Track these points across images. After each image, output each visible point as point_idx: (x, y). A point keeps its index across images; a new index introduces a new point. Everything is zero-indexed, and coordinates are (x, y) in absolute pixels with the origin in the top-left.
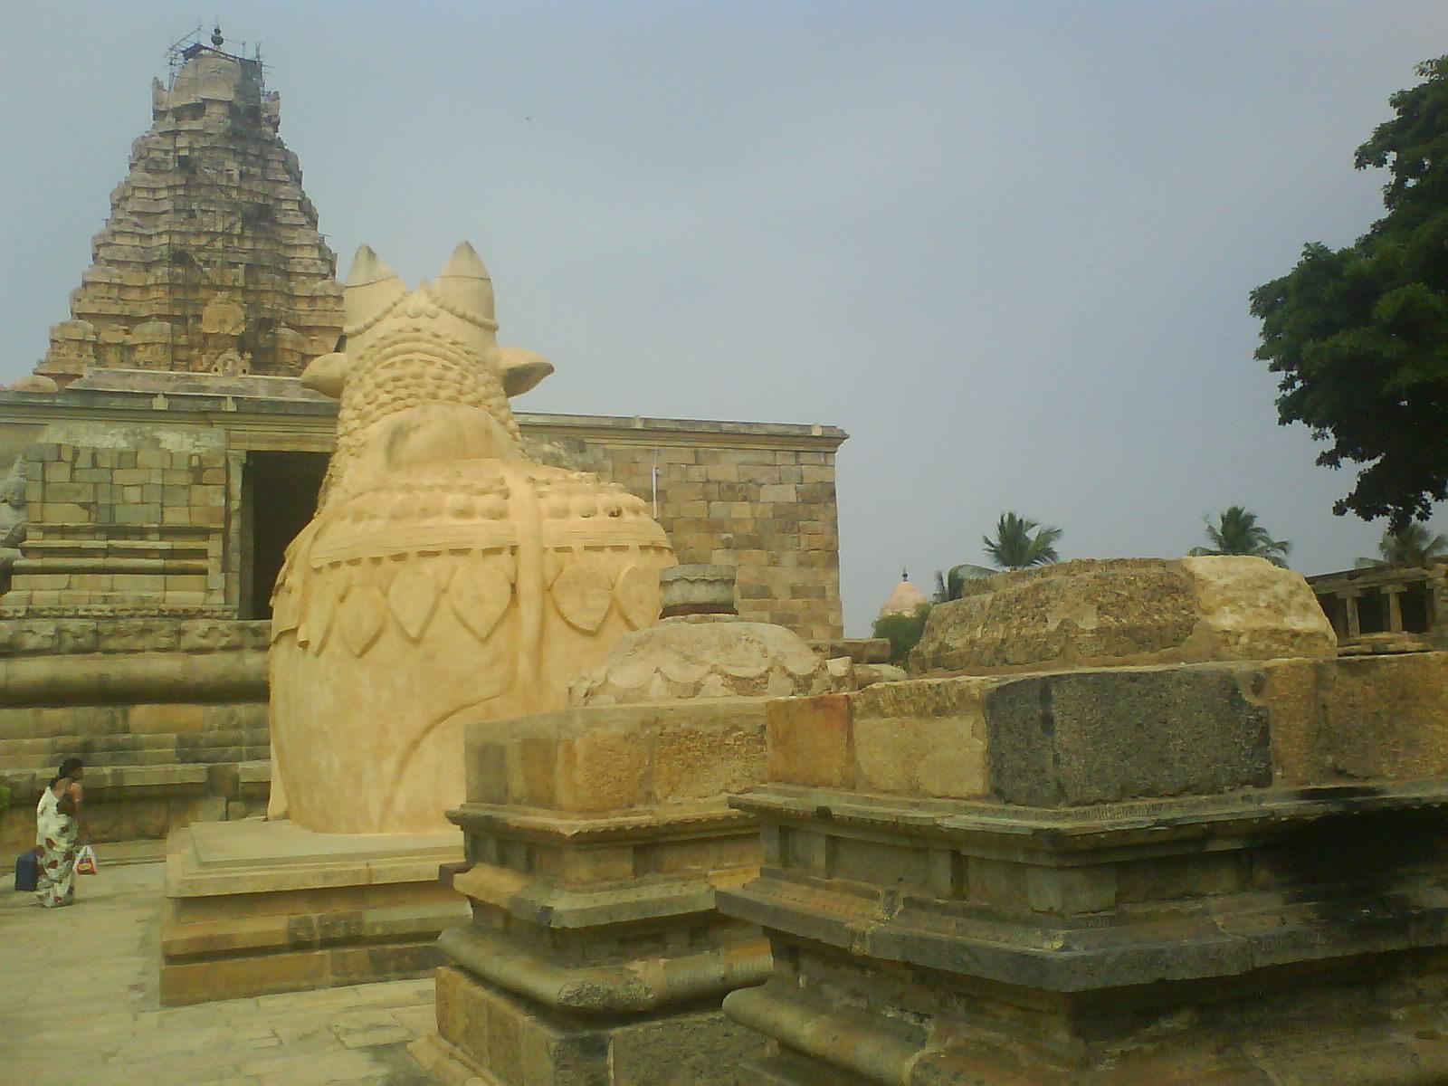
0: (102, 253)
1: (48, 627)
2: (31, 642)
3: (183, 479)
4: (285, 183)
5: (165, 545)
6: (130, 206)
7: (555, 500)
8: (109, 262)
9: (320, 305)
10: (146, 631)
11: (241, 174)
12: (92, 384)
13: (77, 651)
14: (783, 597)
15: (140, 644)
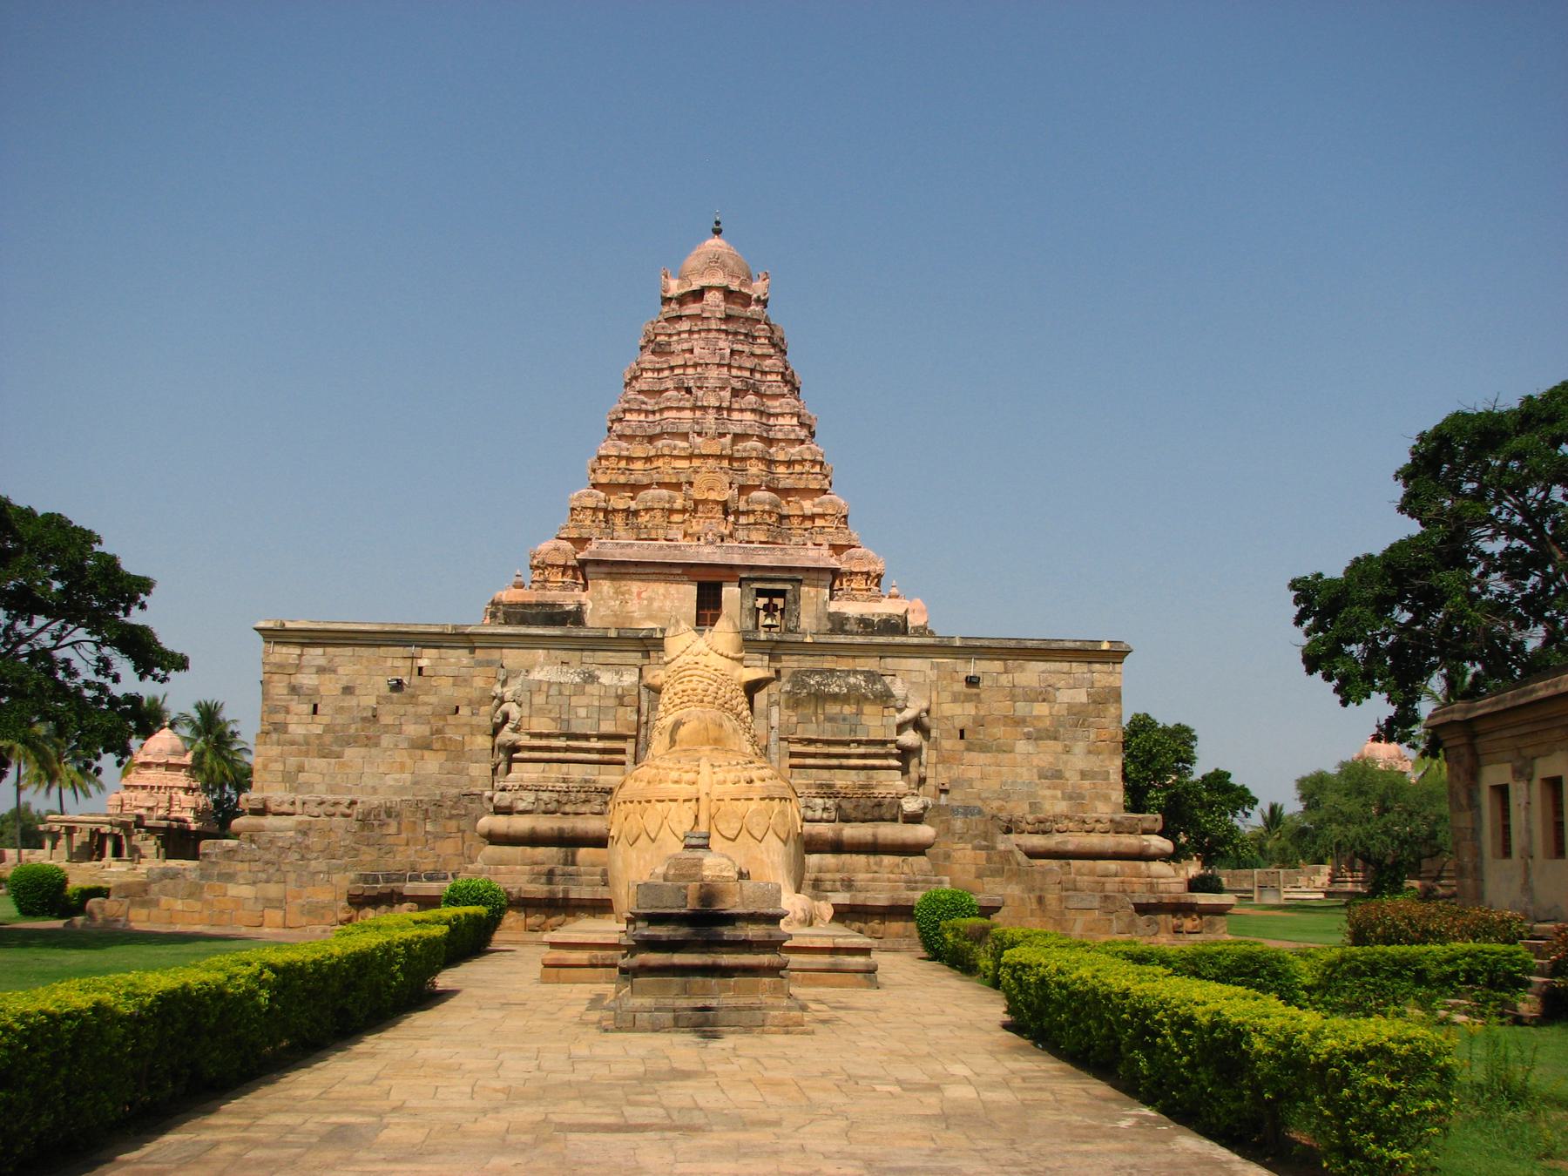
0: (617, 427)
1: (530, 797)
2: (521, 806)
3: (612, 702)
4: (770, 356)
5: (600, 745)
6: (637, 385)
7: (720, 776)
8: (620, 437)
9: (798, 468)
10: (587, 801)
11: (733, 352)
12: (599, 553)
13: (545, 812)
14: (1073, 778)
15: (583, 810)
